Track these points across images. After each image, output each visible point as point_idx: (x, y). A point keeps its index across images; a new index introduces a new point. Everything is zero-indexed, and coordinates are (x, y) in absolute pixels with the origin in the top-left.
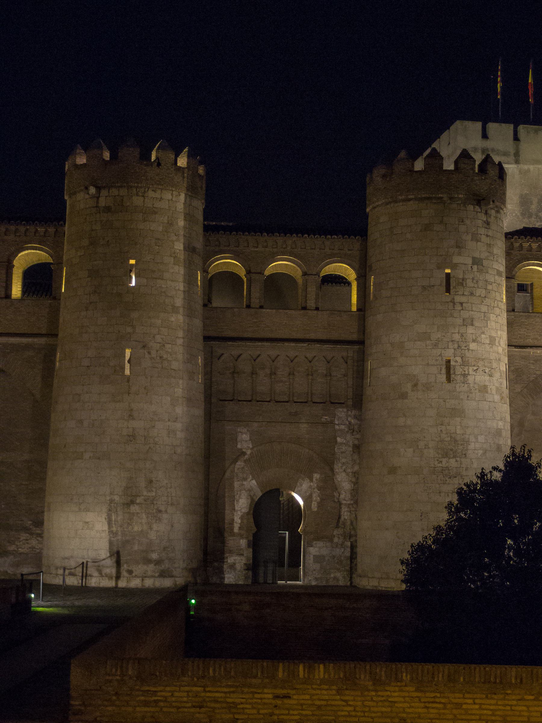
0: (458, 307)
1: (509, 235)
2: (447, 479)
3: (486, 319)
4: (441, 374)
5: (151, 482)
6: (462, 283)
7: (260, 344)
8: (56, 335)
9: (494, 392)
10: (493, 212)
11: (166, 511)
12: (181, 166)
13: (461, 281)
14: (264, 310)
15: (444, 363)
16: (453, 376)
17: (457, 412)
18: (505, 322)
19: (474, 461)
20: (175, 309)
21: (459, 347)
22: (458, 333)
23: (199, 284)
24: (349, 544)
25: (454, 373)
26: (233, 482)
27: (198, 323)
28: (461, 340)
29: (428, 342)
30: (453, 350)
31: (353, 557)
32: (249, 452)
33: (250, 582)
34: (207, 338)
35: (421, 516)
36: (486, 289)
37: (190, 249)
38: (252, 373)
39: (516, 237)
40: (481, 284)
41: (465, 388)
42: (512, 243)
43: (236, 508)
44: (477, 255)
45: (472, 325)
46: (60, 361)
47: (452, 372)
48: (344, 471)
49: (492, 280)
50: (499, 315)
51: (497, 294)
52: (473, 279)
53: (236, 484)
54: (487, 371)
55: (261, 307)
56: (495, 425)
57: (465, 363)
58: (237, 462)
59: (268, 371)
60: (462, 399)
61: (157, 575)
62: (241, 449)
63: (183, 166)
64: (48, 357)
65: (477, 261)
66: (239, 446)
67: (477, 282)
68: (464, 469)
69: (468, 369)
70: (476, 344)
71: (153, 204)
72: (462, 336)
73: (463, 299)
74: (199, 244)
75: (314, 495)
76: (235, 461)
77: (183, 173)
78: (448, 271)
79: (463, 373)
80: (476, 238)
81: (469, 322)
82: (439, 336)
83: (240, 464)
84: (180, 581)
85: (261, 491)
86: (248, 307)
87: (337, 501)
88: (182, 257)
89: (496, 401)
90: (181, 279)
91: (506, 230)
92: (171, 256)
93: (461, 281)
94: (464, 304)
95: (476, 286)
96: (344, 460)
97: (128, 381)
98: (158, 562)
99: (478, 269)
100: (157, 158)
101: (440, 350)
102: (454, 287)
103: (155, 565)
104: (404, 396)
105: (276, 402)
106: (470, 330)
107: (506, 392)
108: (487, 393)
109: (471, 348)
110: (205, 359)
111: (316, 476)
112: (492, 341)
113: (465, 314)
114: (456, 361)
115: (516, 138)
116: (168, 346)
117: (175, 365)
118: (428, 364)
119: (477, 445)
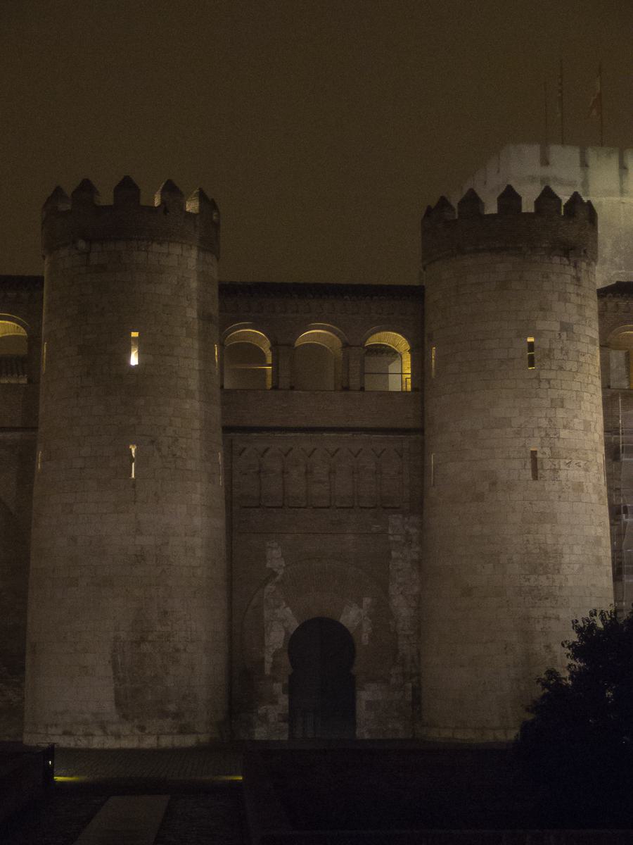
0: (544, 385)
1: (603, 293)
2: (537, 601)
3: (579, 399)
4: (525, 469)
5: (166, 613)
6: (549, 354)
7: (293, 434)
8: (35, 429)
9: (591, 491)
10: (584, 265)
11: (185, 650)
12: (191, 211)
13: (547, 352)
14: (295, 392)
15: (529, 455)
16: (540, 471)
18: (600, 401)
21: (547, 435)
22: (546, 417)
23: (217, 360)
24: (410, 685)
25: (542, 468)
27: (217, 410)
28: (548, 426)
29: (509, 429)
31: (417, 701)
32: (281, 572)
33: (285, 737)
34: (227, 429)
35: (505, 648)
36: (578, 362)
37: (205, 317)
38: (283, 472)
39: (611, 294)
42: (605, 304)
43: (266, 644)
45: (563, 407)
46: (43, 462)
47: (539, 466)
48: (401, 593)
49: (585, 350)
50: (594, 394)
51: (591, 367)
52: (562, 349)
53: (266, 614)
54: (582, 463)
55: (292, 388)
56: (593, 532)
57: (555, 456)
58: (266, 584)
61: (175, 731)
62: (271, 569)
63: (194, 212)
64: (25, 457)
65: (566, 327)
66: (268, 565)
67: (567, 353)
68: (557, 588)
70: (568, 430)
71: (159, 261)
72: (550, 421)
73: (551, 375)
74: (214, 310)
75: (364, 625)
78: (531, 340)
79: (554, 467)
80: (564, 298)
81: (560, 403)
83: (270, 587)
84: (204, 738)
86: (275, 388)
87: (392, 631)
88: (196, 327)
89: (593, 501)
91: (600, 285)
93: (547, 352)
94: (551, 382)
95: (565, 357)
96: (400, 580)
97: (134, 486)
98: (177, 715)
99: (567, 336)
100: (163, 202)
101: (524, 439)
102: (539, 361)
103: (173, 719)
104: (479, 497)
105: (314, 508)
106: (560, 413)
107: (604, 489)
108: (582, 491)
109: (561, 437)
110: (224, 455)
111: (367, 601)
112: (587, 427)
114: (544, 453)
115: (584, 165)
119: (574, 558)
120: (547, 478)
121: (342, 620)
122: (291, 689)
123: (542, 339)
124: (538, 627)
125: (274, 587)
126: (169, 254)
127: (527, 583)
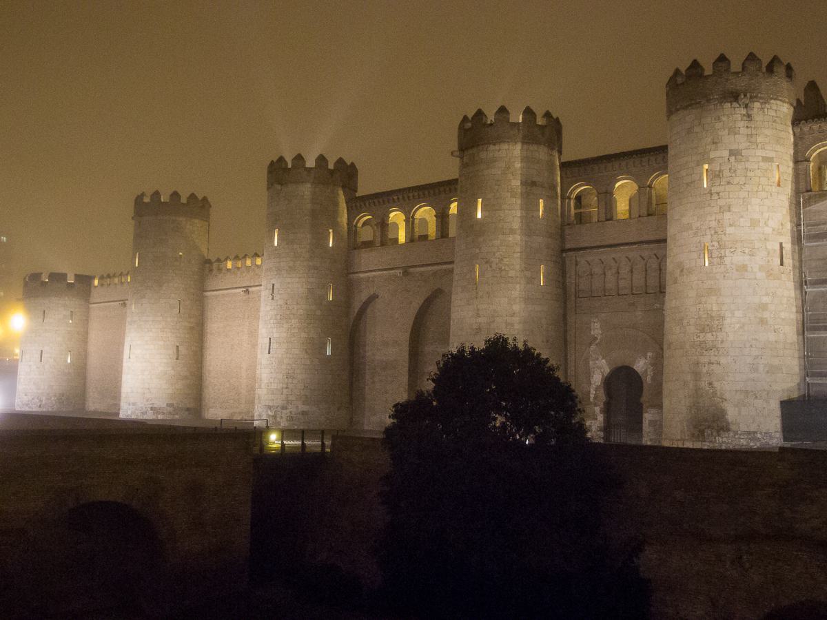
7: (603, 249)
13: (717, 173)
17: (713, 291)
19: (729, 334)
20: (512, 231)
21: (716, 232)
26: (589, 362)
29: (690, 232)
30: (709, 237)
40: (738, 172)
41: (722, 269)
44: (734, 147)
45: (729, 211)
54: (746, 251)
57: (721, 246)
59: (614, 271)
60: (718, 280)
65: (734, 153)
66: (592, 333)
69: (725, 251)
70: (733, 228)
73: (721, 189)
76: (590, 344)
77: (519, 127)
80: (733, 131)
82: (699, 225)
83: (593, 347)
85: (610, 368)
88: (520, 191)
90: (518, 207)
92: (508, 191)
95: (734, 175)
106: (727, 216)
108: (746, 271)
111: (649, 354)
113: (722, 202)
114: (713, 246)
116: (505, 260)
117: (512, 273)
118: (690, 251)
120: (715, 263)
121: (635, 368)
122: (608, 409)
123: (713, 165)
124: (704, 370)
125: (594, 347)
126: (500, 150)
127: (698, 339)
